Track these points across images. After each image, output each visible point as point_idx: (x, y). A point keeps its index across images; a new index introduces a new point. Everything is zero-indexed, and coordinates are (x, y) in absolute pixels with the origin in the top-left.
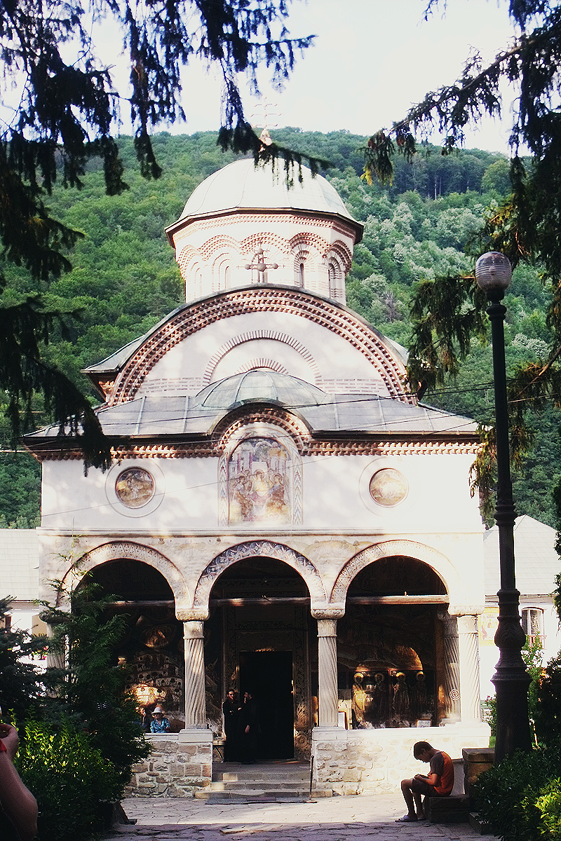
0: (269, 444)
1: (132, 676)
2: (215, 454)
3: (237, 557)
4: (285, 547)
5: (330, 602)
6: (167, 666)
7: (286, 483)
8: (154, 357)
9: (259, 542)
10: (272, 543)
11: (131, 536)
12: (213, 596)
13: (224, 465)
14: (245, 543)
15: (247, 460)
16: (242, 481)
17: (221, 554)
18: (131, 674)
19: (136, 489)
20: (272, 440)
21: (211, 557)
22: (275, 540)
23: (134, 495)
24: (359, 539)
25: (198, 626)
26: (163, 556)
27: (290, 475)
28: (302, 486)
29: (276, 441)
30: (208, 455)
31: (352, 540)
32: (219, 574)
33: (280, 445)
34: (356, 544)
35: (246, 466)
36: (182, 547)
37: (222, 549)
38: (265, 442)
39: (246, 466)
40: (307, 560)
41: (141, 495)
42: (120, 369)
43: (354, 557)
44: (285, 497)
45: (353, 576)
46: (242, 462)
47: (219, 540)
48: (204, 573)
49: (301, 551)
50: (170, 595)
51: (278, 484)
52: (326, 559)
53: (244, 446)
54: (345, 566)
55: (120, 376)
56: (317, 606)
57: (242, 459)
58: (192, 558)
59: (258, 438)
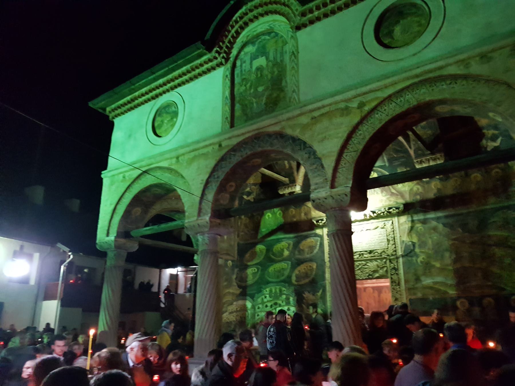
0: (267, 37)
1: (260, 306)
2: (219, 65)
5: (333, 187)
6: (284, 297)
10: (270, 135)
13: (228, 73)
15: (248, 62)
16: (244, 83)
18: (260, 304)
19: (166, 121)
20: (269, 32)
28: (297, 65)
29: (272, 32)
32: (220, 180)
34: (361, 105)
38: (263, 37)
40: (305, 143)
41: (169, 125)
43: (361, 122)
44: (284, 84)
45: (361, 147)
46: (244, 65)
47: (220, 145)
49: (296, 133)
51: (276, 73)
52: (324, 135)
54: (349, 137)
57: (245, 62)
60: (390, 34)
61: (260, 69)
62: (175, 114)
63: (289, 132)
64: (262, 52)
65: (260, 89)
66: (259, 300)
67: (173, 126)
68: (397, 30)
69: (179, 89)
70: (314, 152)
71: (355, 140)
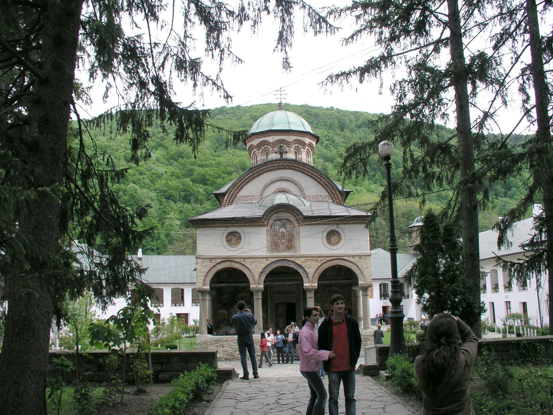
3: (274, 266)
4: (293, 262)
7: (294, 236)
8: (240, 188)
9: (283, 260)
10: (288, 261)
11: (233, 258)
12: (265, 282)
14: (277, 261)
17: (268, 265)
20: (287, 220)
21: (264, 266)
22: (290, 259)
23: (233, 242)
24: (322, 259)
25: (260, 293)
26: (245, 266)
27: (295, 233)
30: (263, 225)
31: (319, 259)
33: (291, 221)
34: (321, 260)
35: (277, 230)
36: (252, 263)
37: (269, 263)
39: (277, 230)
42: (227, 192)
43: (321, 265)
48: (261, 272)
49: (300, 263)
50: (248, 281)
53: (277, 222)
54: (317, 269)
55: (227, 195)
56: (306, 285)
58: (256, 266)
59: (282, 220)
60: (330, 239)
61: (282, 232)
62: (240, 238)
63: (297, 262)
64: (284, 226)
65: (283, 241)
66: (232, 310)
67: (239, 243)
68: (332, 240)
69: (242, 228)
70: (305, 271)
71: (318, 270)
